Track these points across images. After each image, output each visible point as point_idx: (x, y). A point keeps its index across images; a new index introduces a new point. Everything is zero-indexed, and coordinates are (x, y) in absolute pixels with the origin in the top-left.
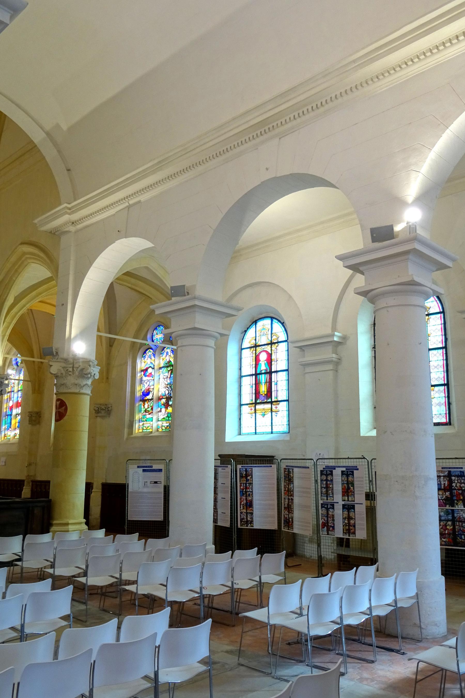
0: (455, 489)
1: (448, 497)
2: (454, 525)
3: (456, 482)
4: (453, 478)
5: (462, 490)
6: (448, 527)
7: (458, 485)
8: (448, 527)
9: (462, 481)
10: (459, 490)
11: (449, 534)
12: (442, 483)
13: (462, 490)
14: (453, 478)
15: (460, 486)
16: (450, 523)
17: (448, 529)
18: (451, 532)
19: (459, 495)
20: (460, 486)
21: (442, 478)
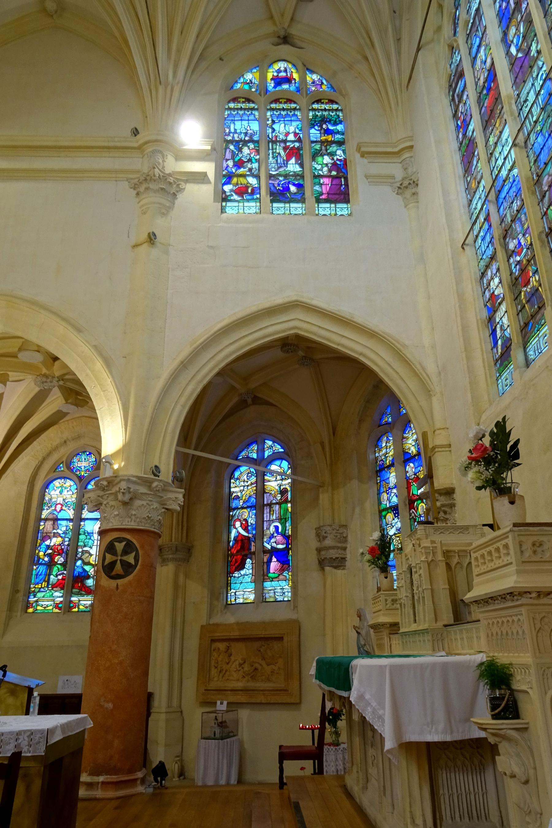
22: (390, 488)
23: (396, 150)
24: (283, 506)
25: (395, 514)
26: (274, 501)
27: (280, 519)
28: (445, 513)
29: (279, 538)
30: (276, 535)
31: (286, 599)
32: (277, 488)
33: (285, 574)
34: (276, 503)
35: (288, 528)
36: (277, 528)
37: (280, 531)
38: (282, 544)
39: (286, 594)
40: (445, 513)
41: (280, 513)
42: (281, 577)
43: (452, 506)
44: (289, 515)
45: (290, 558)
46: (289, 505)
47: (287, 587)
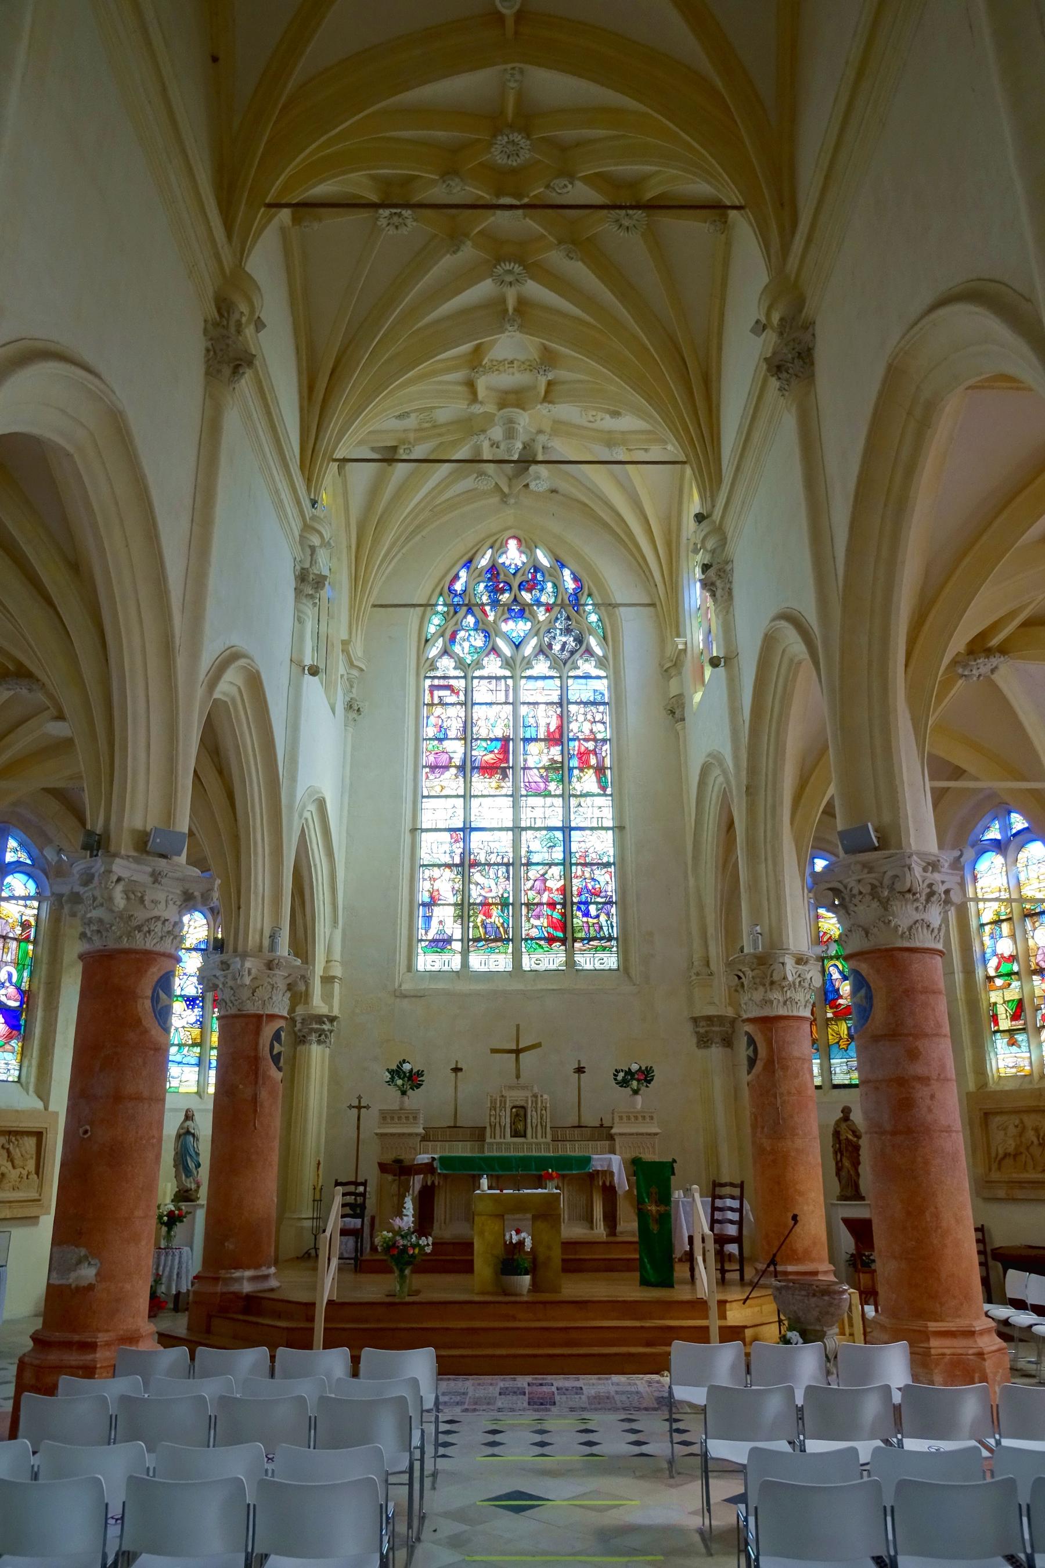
0: (578, 739)
1: (556, 762)
2: (568, 876)
3: (581, 718)
4: (573, 708)
5: (595, 740)
6: (548, 884)
7: (586, 727)
8: (548, 884)
9: (598, 717)
10: (586, 740)
11: (552, 905)
12: (542, 723)
13: (595, 740)
14: (573, 708)
15: (591, 731)
16: (556, 871)
17: (550, 890)
18: (558, 897)
19: (583, 756)
20: (591, 731)
21: (542, 707)
22: (185, 974)
23: (356, 663)
24: (23, 945)
25: (188, 1006)
26: (11, 935)
27: (16, 964)
28: (326, 1036)
29: (12, 990)
30: (7, 984)
31: (10, 1079)
32: (18, 916)
33: (13, 1043)
34: (15, 939)
35: (25, 980)
36: (10, 975)
37: (14, 980)
38: (15, 1000)
39: (12, 1071)
40: (326, 1036)
41: (17, 955)
42: (7, 1047)
43: (331, 1031)
44: (28, 961)
45: (22, 1022)
46: (31, 947)
47: (14, 1062)
